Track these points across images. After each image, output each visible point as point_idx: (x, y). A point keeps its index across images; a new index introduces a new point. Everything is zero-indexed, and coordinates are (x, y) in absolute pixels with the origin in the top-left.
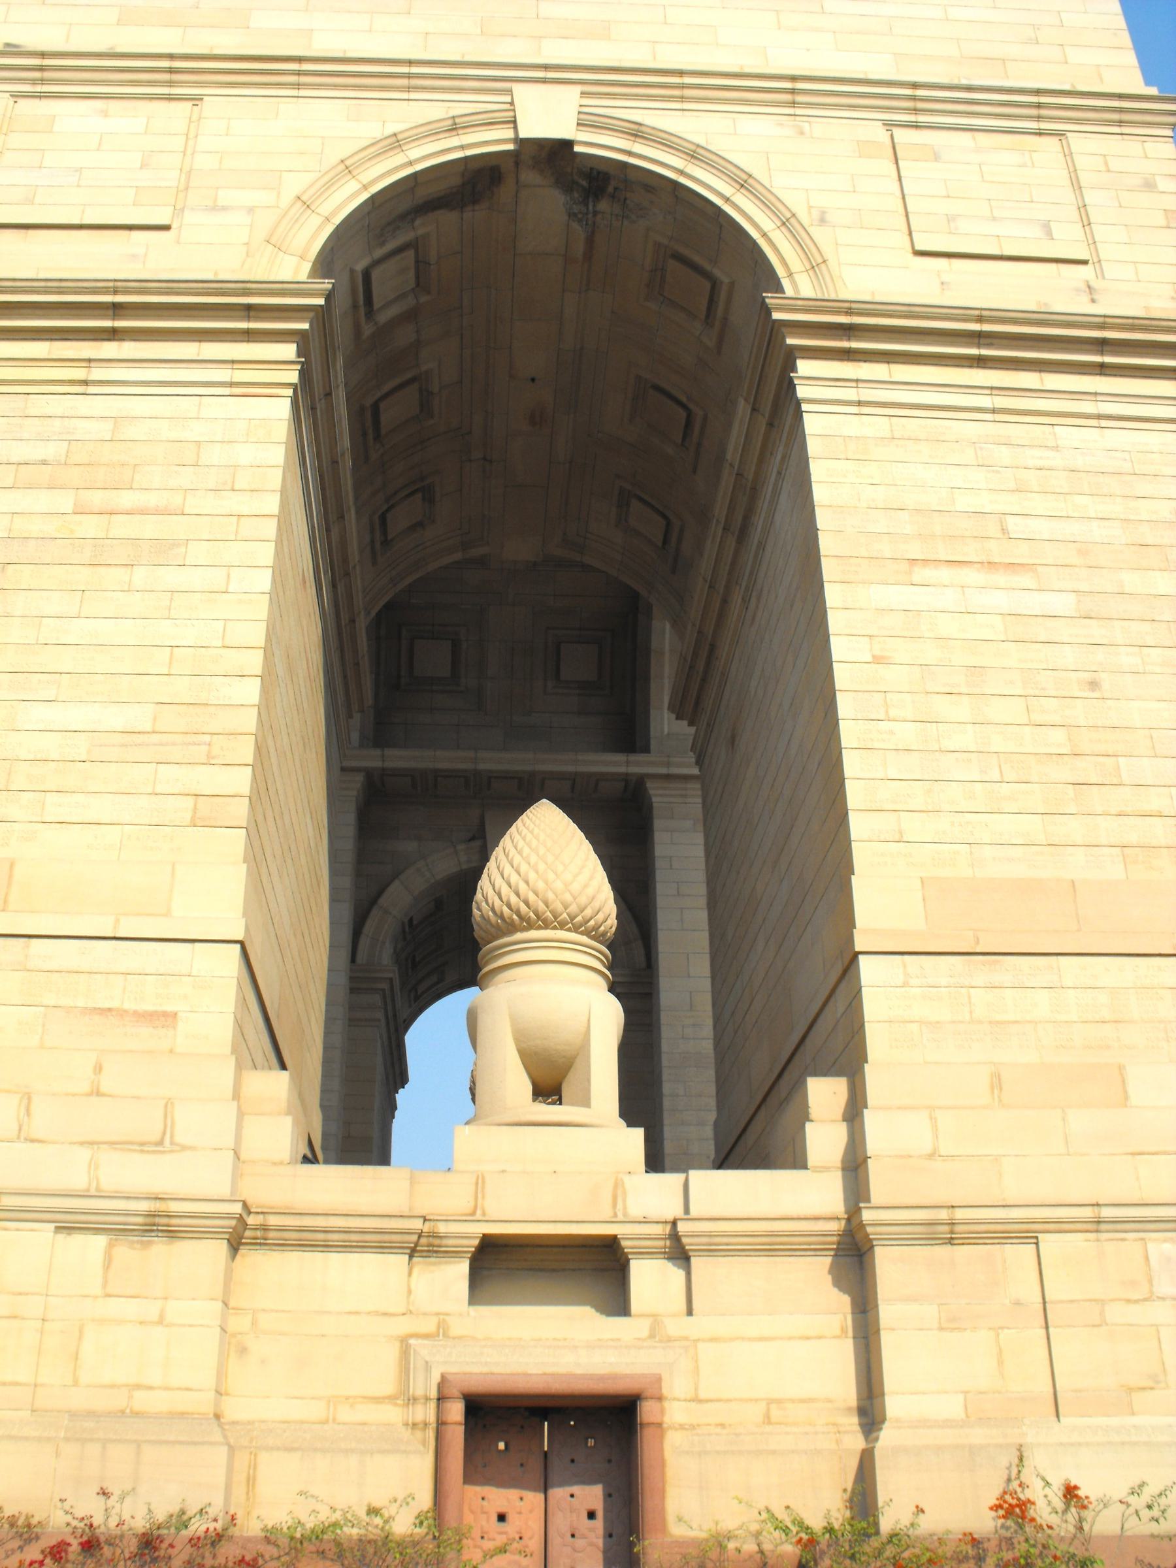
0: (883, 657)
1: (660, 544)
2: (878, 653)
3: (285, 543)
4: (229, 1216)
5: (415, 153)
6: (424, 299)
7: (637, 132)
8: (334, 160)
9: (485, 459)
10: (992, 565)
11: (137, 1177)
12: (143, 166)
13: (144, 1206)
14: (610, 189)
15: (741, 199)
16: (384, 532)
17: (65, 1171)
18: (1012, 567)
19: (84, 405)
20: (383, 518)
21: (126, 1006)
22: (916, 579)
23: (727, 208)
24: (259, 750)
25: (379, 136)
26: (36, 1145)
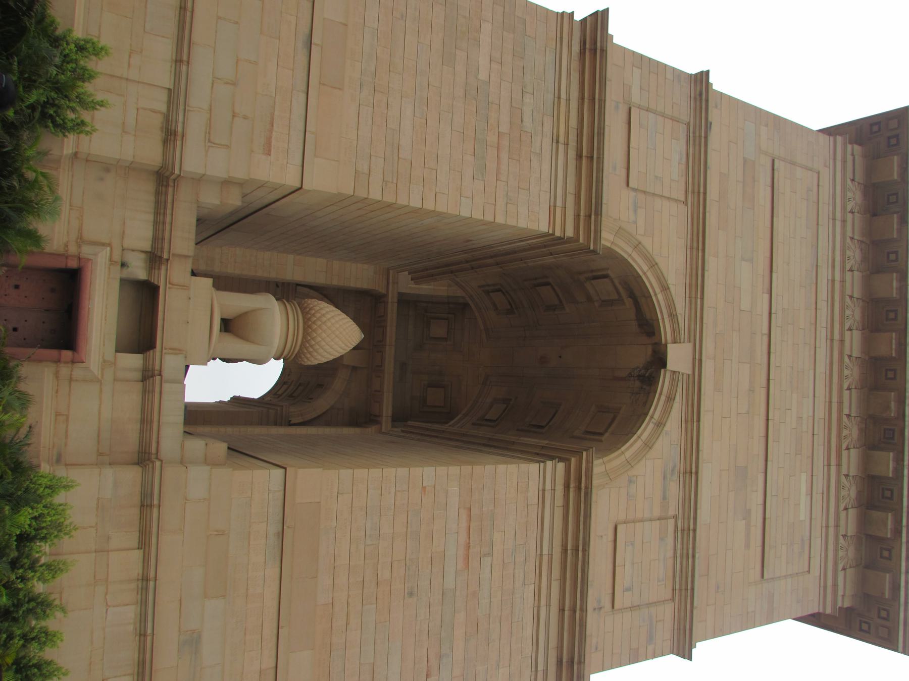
1: (486, 417)
4: (173, 168)
5: (660, 297)
6: (596, 304)
7: (670, 399)
8: (657, 261)
10: (468, 547)
12: (656, 177)
13: (180, 129)
15: (639, 444)
16: (493, 291)
17: (199, 95)
18: (467, 557)
19: (547, 141)
20: (499, 290)
21: (274, 133)
24: (390, 205)
25: (669, 282)
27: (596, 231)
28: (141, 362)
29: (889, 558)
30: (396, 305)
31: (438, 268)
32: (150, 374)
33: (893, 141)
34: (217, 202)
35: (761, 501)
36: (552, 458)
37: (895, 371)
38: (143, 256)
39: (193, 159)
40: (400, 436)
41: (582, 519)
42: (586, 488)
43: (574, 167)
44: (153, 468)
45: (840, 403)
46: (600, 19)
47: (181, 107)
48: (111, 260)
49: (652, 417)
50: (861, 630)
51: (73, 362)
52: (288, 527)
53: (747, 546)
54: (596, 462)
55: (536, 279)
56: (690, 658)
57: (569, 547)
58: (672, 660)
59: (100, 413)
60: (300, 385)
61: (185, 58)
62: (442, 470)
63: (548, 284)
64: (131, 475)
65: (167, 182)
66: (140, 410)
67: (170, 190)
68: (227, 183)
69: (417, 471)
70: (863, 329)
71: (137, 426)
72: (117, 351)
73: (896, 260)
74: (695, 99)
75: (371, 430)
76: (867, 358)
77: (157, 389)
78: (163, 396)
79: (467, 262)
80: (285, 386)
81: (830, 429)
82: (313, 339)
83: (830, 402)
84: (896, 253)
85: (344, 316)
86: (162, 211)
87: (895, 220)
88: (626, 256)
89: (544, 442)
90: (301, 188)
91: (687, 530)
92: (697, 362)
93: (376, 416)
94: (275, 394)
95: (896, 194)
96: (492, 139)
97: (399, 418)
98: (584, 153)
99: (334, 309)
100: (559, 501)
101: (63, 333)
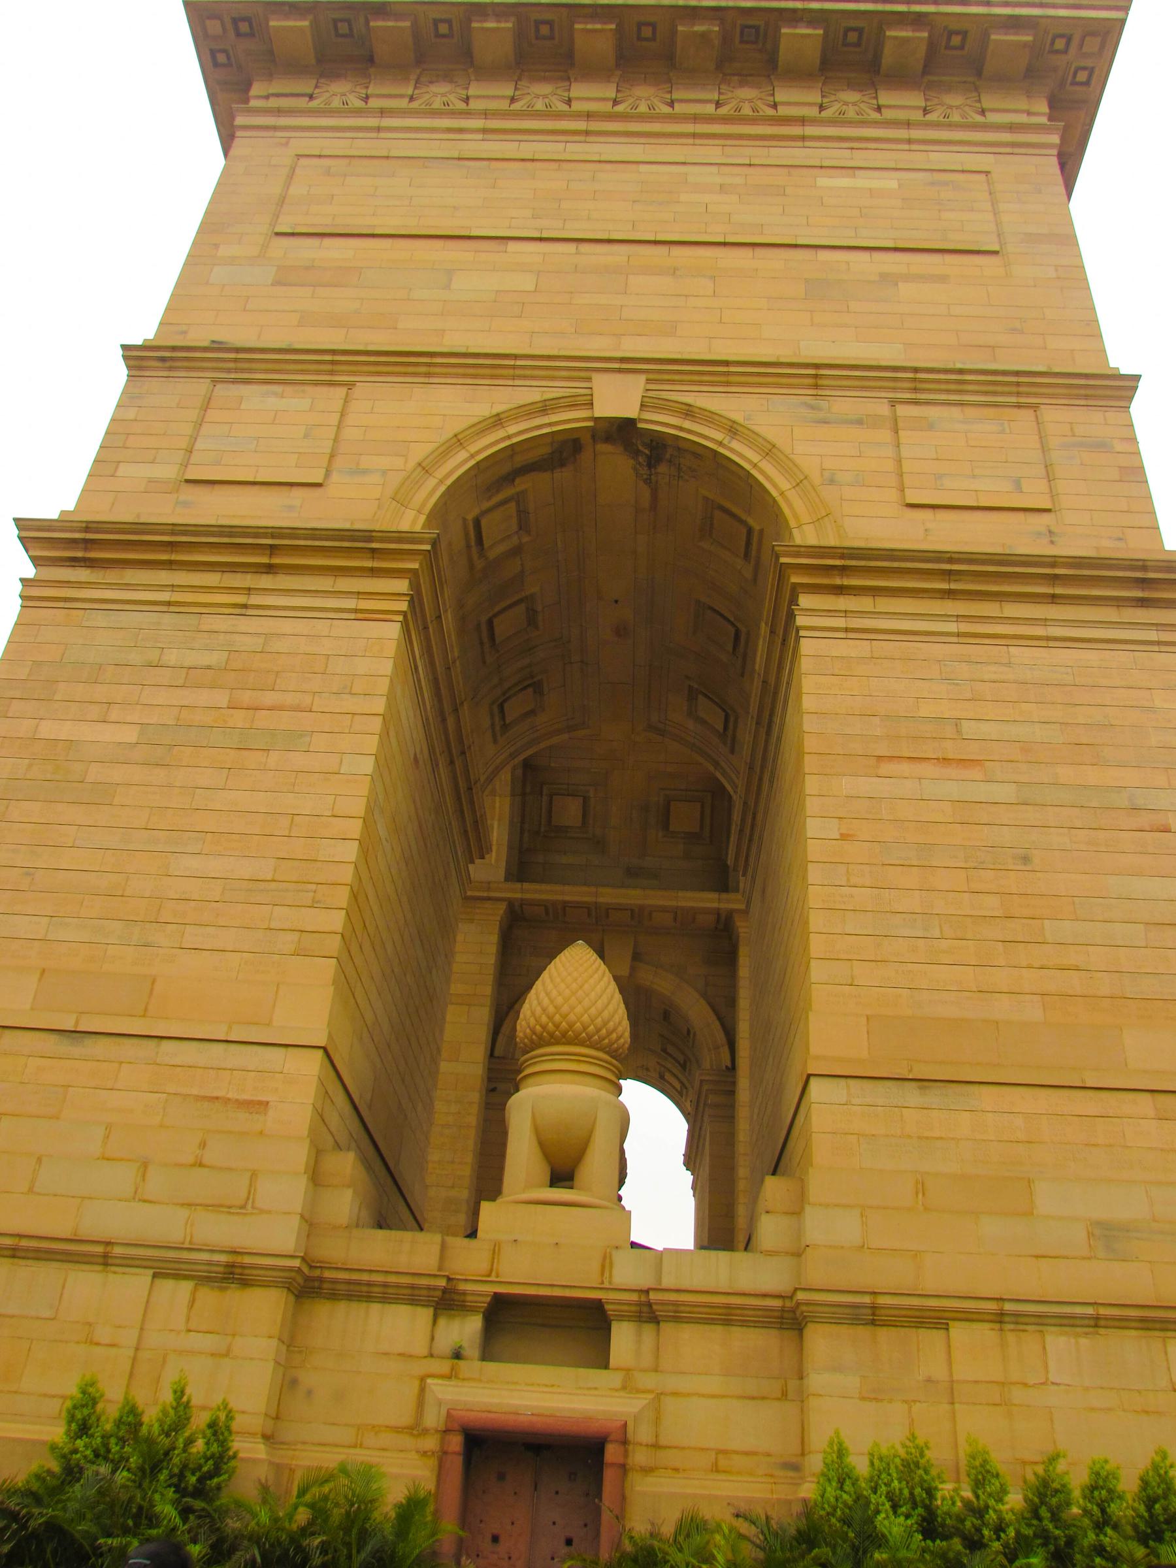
0: (848, 835)
2: (844, 831)
3: (392, 733)
5: (512, 429)
6: (526, 539)
7: (689, 412)
8: (451, 435)
9: (582, 662)
10: (946, 761)
11: (221, 1233)
12: (306, 436)
13: (223, 1258)
14: (668, 456)
15: (766, 465)
16: (503, 718)
17: (165, 1224)
18: (962, 762)
19: (244, 624)
20: (501, 707)
21: (230, 1095)
22: (882, 772)
23: (754, 472)
24: (354, 896)
25: (487, 414)
26: (147, 1204)
27: (399, 540)
28: (625, 1324)
29: (964, 34)
30: (526, 885)
31: (462, 812)
32: (645, 1309)
33: (244, 27)
34: (348, 1194)
35: (864, 256)
36: (791, 616)
37: (640, 25)
38: (442, 1322)
39: (276, 1236)
40: (754, 879)
41: (896, 564)
42: (842, 557)
43: (288, 578)
44: (808, 1303)
45: (695, 119)
46: (33, 534)
47: (185, 1255)
48: (449, 1377)
49: (720, 444)
50: (1087, 84)
51: (625, 1442)
52: (910, 1071)
53: (943, 279)
54: (798, 541)
55: (482, 643)
56: (1137, 378)
57: (1140, 594)
58: (1140, 408)
59: (713, 1396)
60: (664, 1050)
61: (100, 1249)
62: (812, 805)
63: (490, 623)
64: (821, 1341)
65: (313, 1279)
66: (706, 1327)
67: (327, 1274)
68: (316, 1177)
69: (814, 850)
70: (569, 79)
71: (736, 1331)
72: (606, 1366)
73: (449, 22)
74: (170, 369)
75: (743, 928)
76: (619, 73)
77: (673, 1297)
78: (683, 1287)
79: (452, 762)
80: (667, 1076)
81: (740, 137)
82: (585, 1028)
83: (694, 136)
84: (436, 22)
85: (545, 975)
86: (365, 1289)
87: (380, 23)
88: (443, 488)
89: (764, 629)
90: (325, 1049)
91: (914, 384)
92: (626, 365)
93: (718, 921)
94: (681, 1094)
95: (335, 21)
96: (239, 718)
97: (721, 878)
98: (265, 560)
99: (533, 991)
100: (865, 603)
101: (576, 1459)
